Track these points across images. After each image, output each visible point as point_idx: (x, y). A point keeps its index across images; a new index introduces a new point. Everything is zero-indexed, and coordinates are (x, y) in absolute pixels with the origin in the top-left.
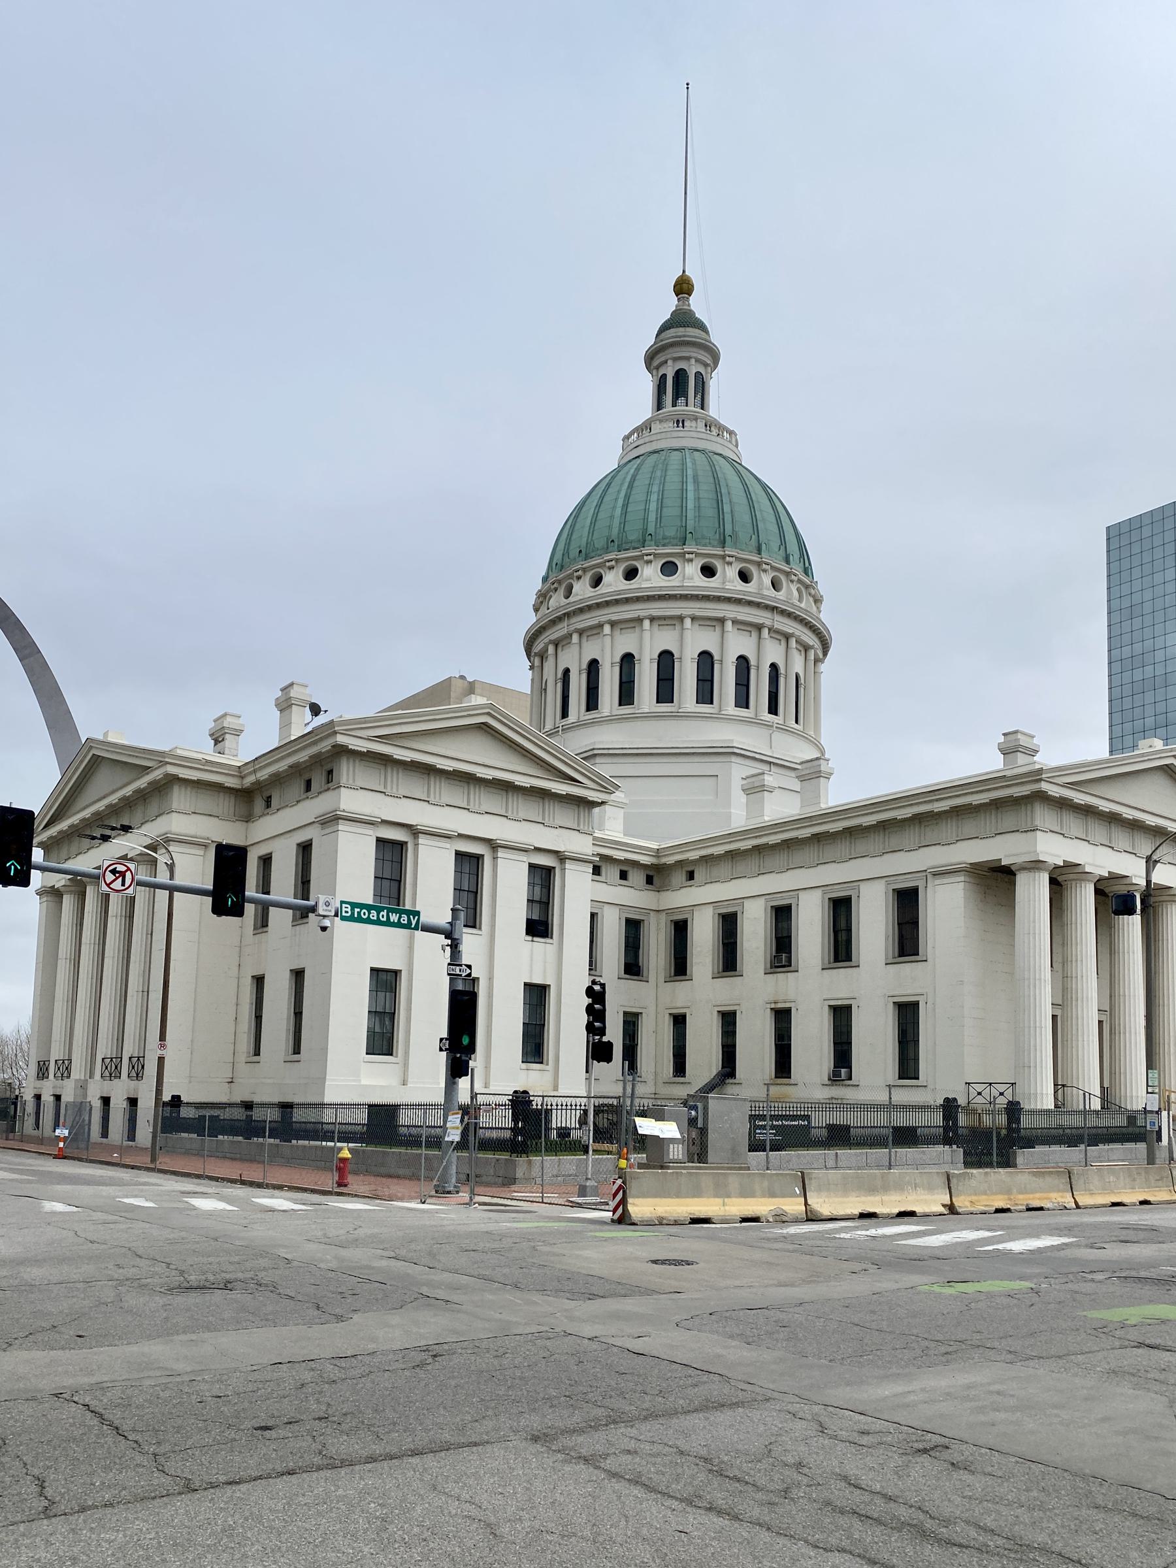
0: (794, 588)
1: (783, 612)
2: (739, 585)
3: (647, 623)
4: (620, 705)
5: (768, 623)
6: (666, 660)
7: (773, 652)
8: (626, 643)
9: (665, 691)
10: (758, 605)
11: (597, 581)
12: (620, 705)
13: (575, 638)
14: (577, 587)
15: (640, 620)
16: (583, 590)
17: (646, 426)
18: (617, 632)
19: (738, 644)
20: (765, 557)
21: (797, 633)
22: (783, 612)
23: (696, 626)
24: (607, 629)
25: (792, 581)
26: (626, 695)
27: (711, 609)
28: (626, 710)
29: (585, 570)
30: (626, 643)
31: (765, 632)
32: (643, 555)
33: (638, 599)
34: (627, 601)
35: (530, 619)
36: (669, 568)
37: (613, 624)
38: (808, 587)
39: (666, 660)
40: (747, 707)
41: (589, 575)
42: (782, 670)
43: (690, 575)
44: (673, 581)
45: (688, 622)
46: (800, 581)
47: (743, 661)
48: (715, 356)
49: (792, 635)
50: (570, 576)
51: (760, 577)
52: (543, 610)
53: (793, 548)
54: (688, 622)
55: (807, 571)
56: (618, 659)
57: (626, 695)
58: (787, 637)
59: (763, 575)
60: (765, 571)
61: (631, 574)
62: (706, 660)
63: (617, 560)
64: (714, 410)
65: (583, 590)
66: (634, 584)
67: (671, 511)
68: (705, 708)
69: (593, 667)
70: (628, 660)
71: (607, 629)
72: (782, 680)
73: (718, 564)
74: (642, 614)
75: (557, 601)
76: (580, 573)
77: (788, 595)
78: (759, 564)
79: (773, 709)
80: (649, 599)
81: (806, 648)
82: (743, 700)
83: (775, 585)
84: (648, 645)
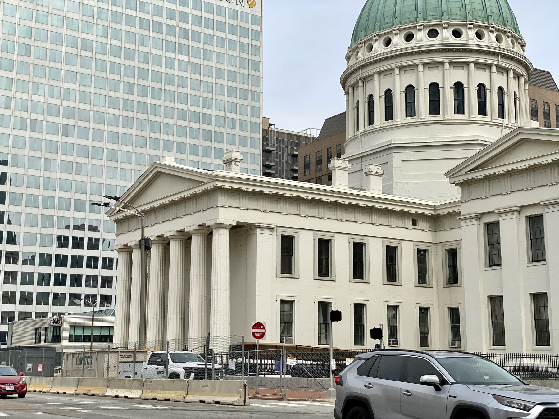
0: (509, 40)
1: (504, 56)
2: (476, 41)
3: (421, 68)
4: (406, 117)
5: (496, 63)
6: (434, 89)
8: (409, 79)
9: (435, 108)
10: (489, 53)
11: (388, 42)
12: (406, 117)
13: (376, 77)
14: (376, 46)
15: (416, 65)
18: (403, 72)
20: (491, 22)
21: (514, 68)
22: (504, 56)
23: (452, 69)
24: (397, 71)
25: (508, 37)
26: (410, 109)
27: (460, 56)
28: (411, 120)
29: (380, 36)
31: (494, 68)
32: (416, 26)
33: (417, 53)
34: (410, 54)
36: (433, 33)
37: (400, 68)
38: (517, 39)
39: (434, 89)
40: (485, 114)
41: (382, 39)
42: (506, 91)
43: (446, 36)
44: (436, 41)
45: (447, 65)
46: (513, 36)
47: (481, 87)
49: (511, 69)
50: (371, 39)
51: (489, 35)
52: (351, 63)
53: (507, 15)
54: (447, 65)
55: (517, 30)
56: (404, 90)
57: (410, 109)
58: (507, 70)
59: (491, 34)
60: (492, 31)
61: (409, 37)
62: (459, 87)
63: (400, 30)
66: (412, 44)
68: (460, 117)
69: (388, 94)
70: (410, 90)
71: (397, 71)
72: (506, 97)
73: (463, 30)
74: (418, 61)
75: (363, 55)
76: (377, 37)
77: (506, 44)
78: (487, 28)
79: (502, 115)
80: (423, 52)
81: (517, 76)
82: (482, 110)
83: (498, 39)
84: (423, 80)
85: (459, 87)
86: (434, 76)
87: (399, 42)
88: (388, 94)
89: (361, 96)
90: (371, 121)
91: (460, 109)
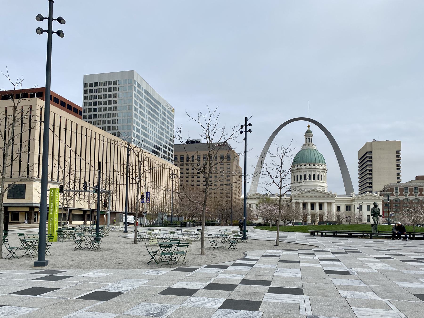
6: (310, 175)
7: (322, 174)
9: (310, 179)
11: (301, 166)
17: (305, 145)
19: (318, 173)
30: (305, 173)
36: (310, 165)
47: (318, 175)
55: (325, 163)
61: (305, 165)
62: (314, 175)
65: (299, 167)
67: (310, 158)
68: (314, 181)
69: (301, 176)
82: (318, 180)
86: (309, 173)
87: (303, 166)
88: (301, 176)
89: (295, 175)
90: (297, 180)
91: (314, 179)
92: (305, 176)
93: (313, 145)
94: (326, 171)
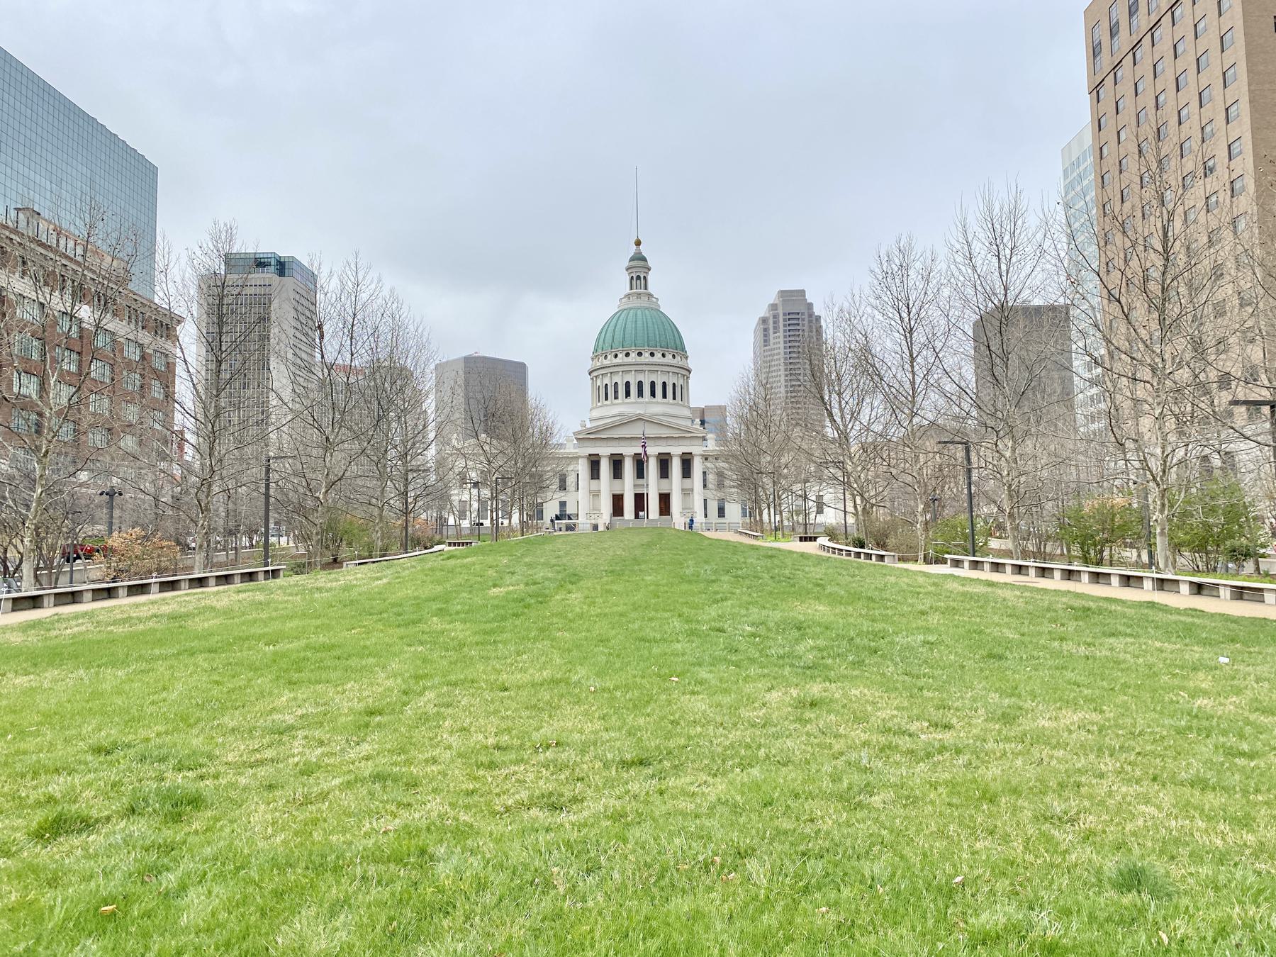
6: (640, 384)
9: (640, 394)
11: (616, 356)
16: (611, 360)
26: (628, 394)
30: (628, 378)
35: (590, 365)
36: (640, 354)
39: (640, 384)
47: (664, 384)
48: (649, 269)
55: (683, 349)
57: (628, 394)
61: (628, 355)
62: (653, 384)
64: (651, 289)
75: (602, 362)
85: (653, 384)
91: (653, 394)
92: (628, 384)
93: (650, 295)
94: (685, 372)
